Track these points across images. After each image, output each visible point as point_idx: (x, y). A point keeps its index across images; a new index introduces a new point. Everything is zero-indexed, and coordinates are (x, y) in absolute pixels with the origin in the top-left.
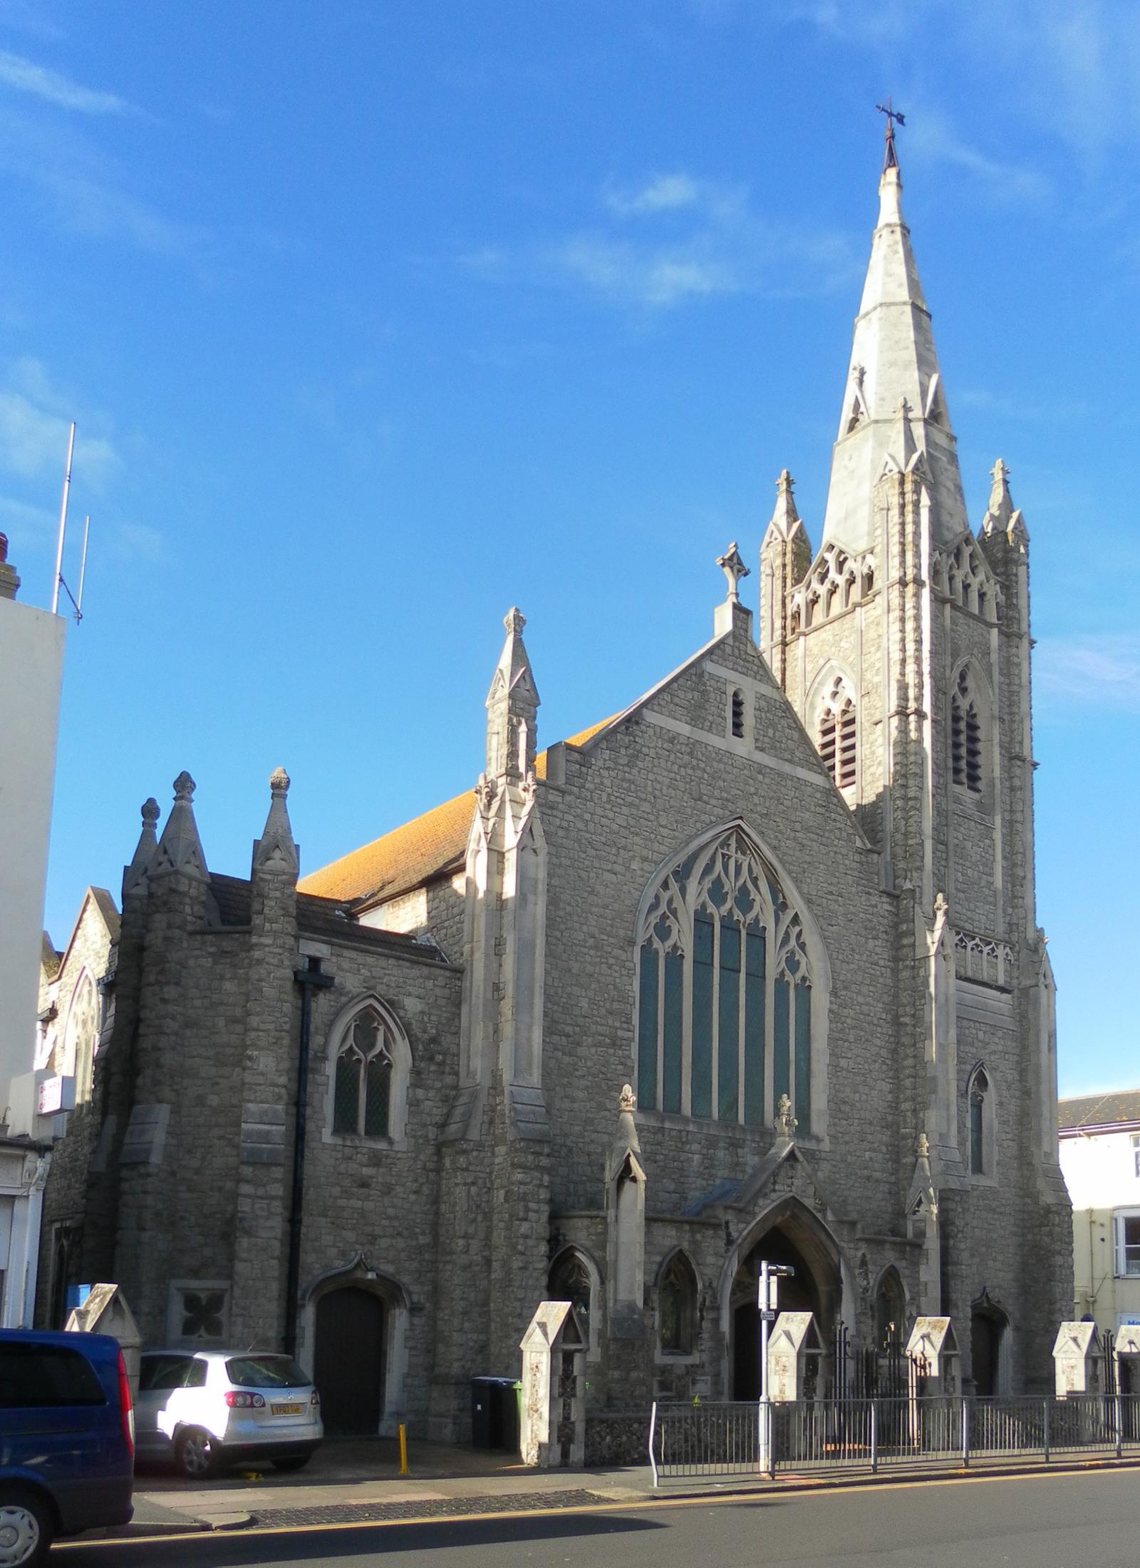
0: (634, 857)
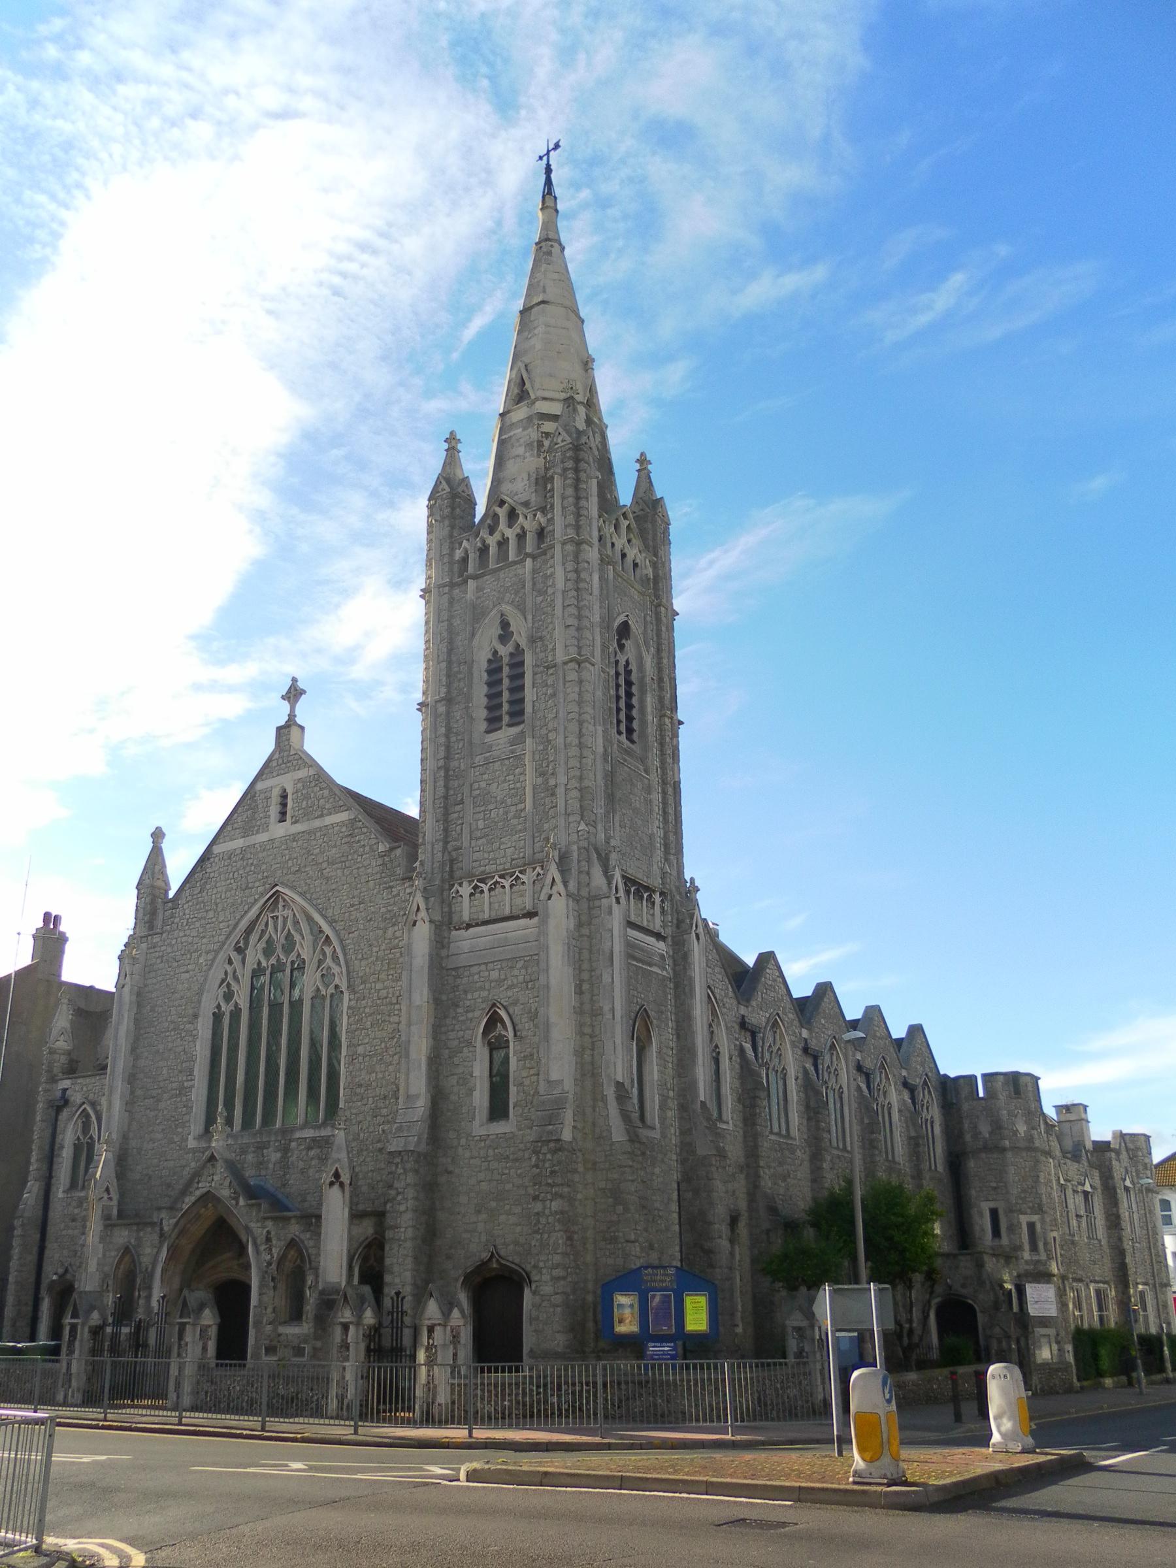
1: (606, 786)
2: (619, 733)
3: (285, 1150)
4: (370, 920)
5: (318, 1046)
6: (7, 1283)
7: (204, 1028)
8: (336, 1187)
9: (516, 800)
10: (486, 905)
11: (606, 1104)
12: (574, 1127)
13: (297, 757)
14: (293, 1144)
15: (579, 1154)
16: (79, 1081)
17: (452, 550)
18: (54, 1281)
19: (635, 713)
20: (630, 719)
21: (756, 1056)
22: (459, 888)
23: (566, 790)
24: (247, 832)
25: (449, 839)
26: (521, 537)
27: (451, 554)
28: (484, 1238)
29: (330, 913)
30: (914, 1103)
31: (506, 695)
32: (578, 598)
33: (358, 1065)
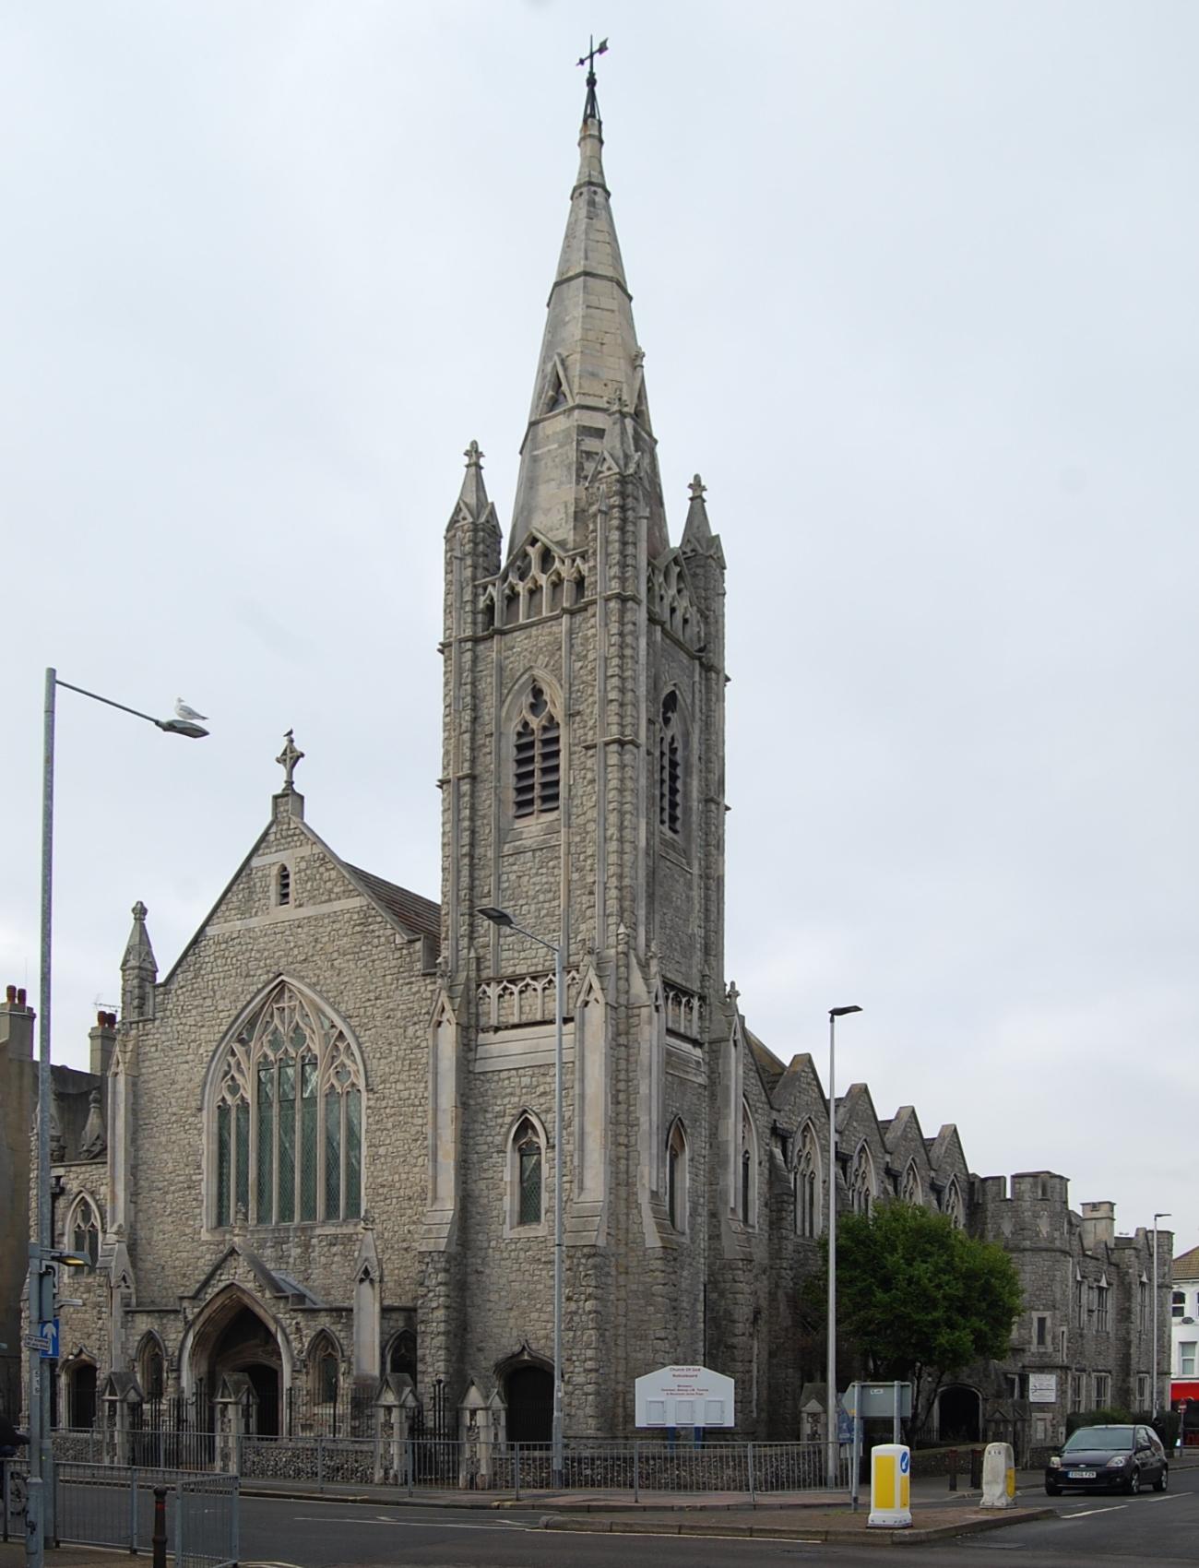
0: (200, 1045)
1: (648, 885)
2: (662, 822)
3: (307, 1246)
4: (389, 1017)
5: (335, 1144)
6: (21, 1361)
7: (208, 1120)
8: (367, 1283)
9: (550, 895)
10: (513, 1008)
11: (640, 1212)
12: (608, 1234)
13: (298, 831)
14: (314, 1241)
15: (613, 1259)
16: (73, 1169)
17: (476, 596)
18: (68, 1360)
19: (679, 798)
20: (673, 805)
21: (786, 1161)
22: (487, 989)
23: (605, 888)
24: (245, 913)
25: (476, 935)
26: (556, 585)
27: (474, 601)
28: (515, 1333)
29: (343, 1007)
30: (940, 1204)
31: (538, 779)
32: (621, 667)
33: (379, 1167)
